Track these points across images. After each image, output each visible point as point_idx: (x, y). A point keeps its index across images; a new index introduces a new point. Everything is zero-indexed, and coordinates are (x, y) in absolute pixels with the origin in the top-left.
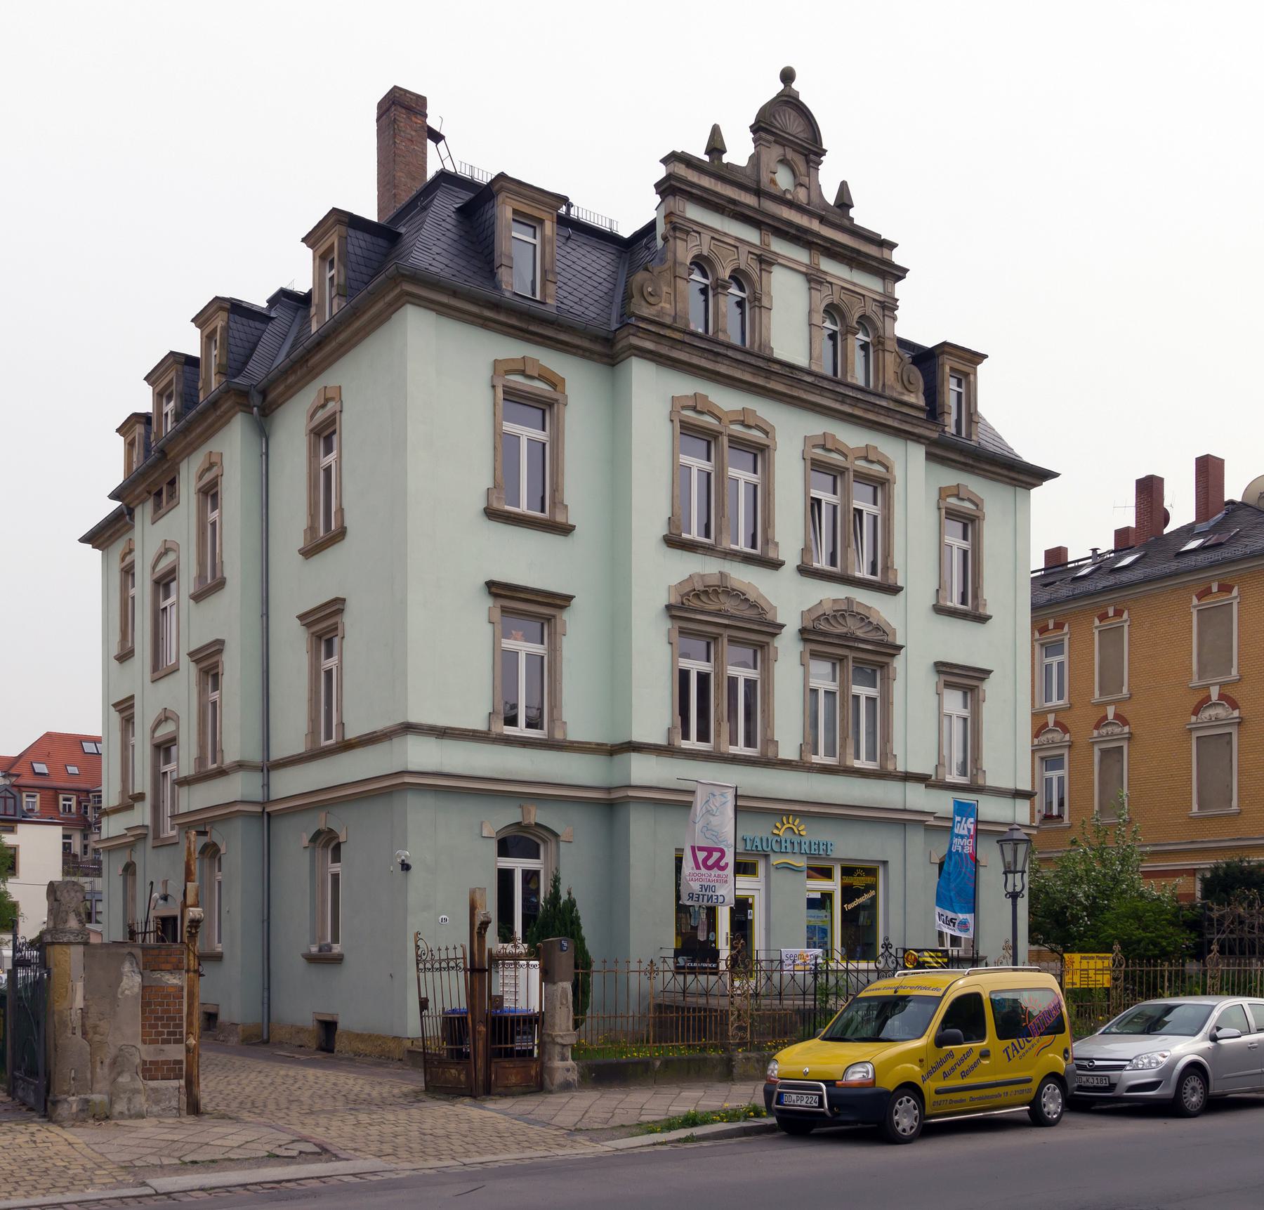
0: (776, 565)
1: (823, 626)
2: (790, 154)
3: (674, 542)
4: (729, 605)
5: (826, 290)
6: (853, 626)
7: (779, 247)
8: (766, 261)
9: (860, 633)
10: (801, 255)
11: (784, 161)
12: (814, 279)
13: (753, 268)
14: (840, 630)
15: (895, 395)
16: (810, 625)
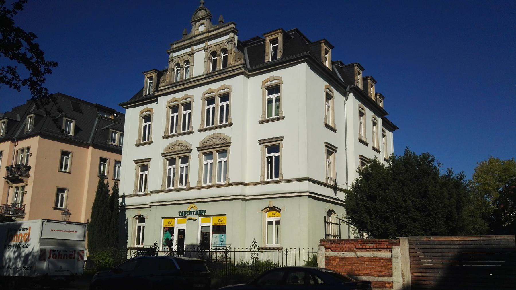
0: (192, 132)
1: (205, 144)
2: (201, 21)
3: (165, 137)
4: (179, 148)
5: (210, 49)
6: (215, 141)
7: (195, 48)
8: (192, 54)
9: (218, 142)
10: (203, 45)
11: (201, 24)
12: (205, 49)
13: (189, 58)
14: (211, 144)
15: (233, 65)
16: (202, 145)
